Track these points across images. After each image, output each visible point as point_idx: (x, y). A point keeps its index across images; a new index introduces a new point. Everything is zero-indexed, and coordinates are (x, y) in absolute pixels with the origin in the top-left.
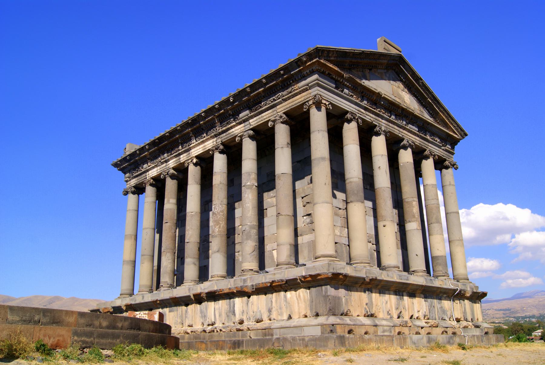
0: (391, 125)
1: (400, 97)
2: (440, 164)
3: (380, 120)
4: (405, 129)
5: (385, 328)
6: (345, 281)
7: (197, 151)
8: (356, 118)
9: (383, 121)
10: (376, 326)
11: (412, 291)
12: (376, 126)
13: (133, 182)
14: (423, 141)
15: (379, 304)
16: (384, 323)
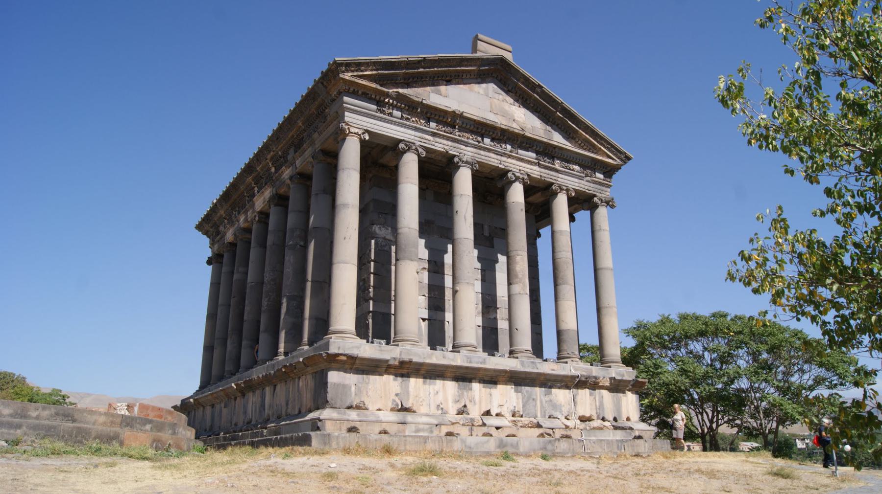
0: (482, 152)
1: (505, 114)
2: (581, 202)
3: (463, 147)
4: (510, 156)
5: (421, 426)
7: (259, 203)
8: (414, 147)
11: (491, 379)
12: (455, 156)
13: (216, 247)
14: (547, 171)
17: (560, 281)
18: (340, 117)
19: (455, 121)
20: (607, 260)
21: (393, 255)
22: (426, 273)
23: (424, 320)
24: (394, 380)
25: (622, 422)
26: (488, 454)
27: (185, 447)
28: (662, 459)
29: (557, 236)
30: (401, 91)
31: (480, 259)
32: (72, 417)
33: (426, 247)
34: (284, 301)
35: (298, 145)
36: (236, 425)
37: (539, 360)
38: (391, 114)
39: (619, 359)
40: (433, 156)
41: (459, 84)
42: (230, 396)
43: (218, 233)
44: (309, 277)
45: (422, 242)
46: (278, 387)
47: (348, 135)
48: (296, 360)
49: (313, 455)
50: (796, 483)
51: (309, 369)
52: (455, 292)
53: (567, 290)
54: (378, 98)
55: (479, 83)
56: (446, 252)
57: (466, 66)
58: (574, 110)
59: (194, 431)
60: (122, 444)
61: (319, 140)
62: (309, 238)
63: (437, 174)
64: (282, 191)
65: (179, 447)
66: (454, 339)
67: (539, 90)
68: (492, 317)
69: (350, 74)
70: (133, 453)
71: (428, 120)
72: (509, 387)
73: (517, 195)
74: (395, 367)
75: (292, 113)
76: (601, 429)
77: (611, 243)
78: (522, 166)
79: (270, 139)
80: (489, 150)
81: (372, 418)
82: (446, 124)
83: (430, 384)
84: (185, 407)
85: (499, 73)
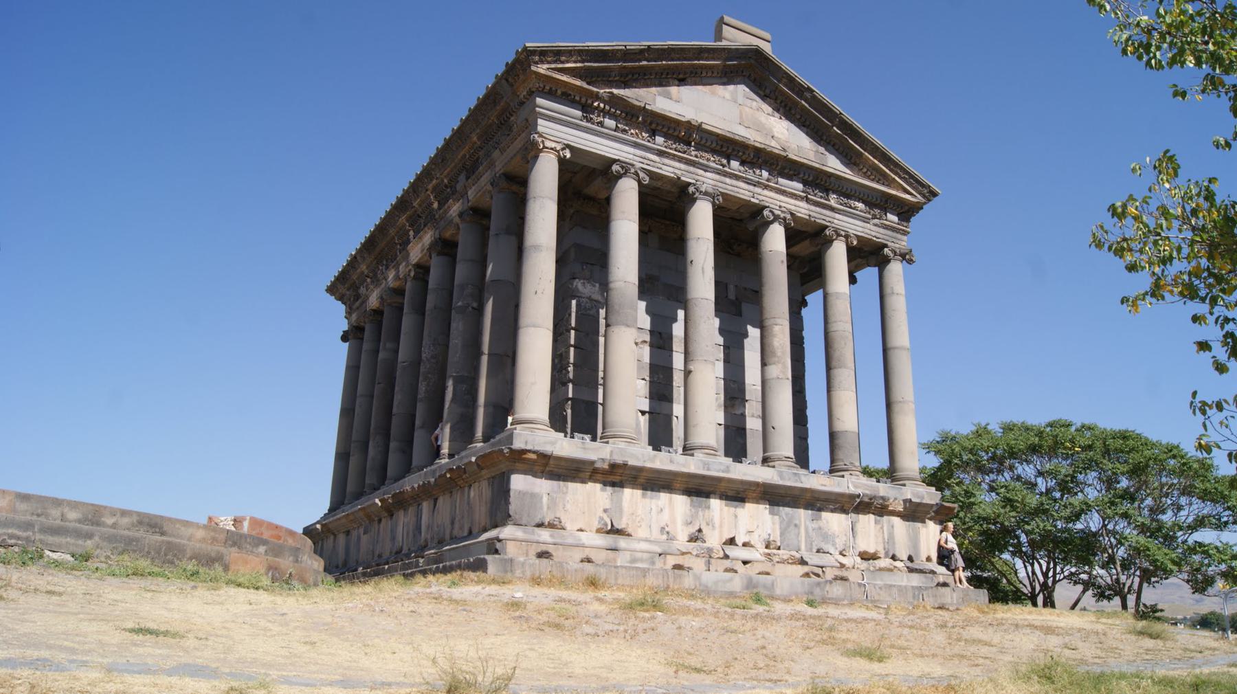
0: (728, 180)
1: (760, 128)
2: (866, 255)
3: (701, 172)
4: (766, 187)
5: (639, 555)
6: (546, 465)
7: (416, 252)
9: (708, 174)
10: (615, 550)
11: (737, 494)
12: (689, 184)
13: (354, 316)
14: (818, 209)
15: (640, 512)
16: (644, 546)
17: (834, 364)
18: (531, 126)
19: (691, 135)
20: (901, 335)
21: (602, 322)
22: (647, 349)
23: (643, 413)
24: (602, 490)
25: (920, 563)
26: (731, 594)
27: (311, 581)
28: (976, 614)
29: (831, 299)
30: (615, 91)
31: (722, 331)
32: (161, 528)
33: (648, 312)
34: (450, 383)
35: (471, 169)
36: (380, 556)
37: (803, 472)
38: (601, 124)
39: (916, 474)
40: (659, 184)
41: (696, 84)
42: (372, 518)
43: (357, 297)
44: (486, 348)
45: (642, 305)
46: (440, 501)
47: (541, 151)
48: (466, 461)
49: (489, 584)
50: (1169, 644)
51: (484, 472)
52: (687, 373)
53: (844, 376)
54: (583, 100)
55: (724, 84)
56: (676, 320)
57: (707, 59)
58: (857, 124)
59: (322, 563)
60: (226, 568)
61: (501, 161)
62: (486, 295)
63: (664, 211)
64: (447, 234)
65: (303, 580)
66: (686, 439)
67: (808, 95)
68: (739, 412)
69: (546, 66)
70: (241, 580)
71: (653, 133)
72: (761, 507)
73: (775, 241)
74: (604, 473)
75: (464, 123)
76: (890, 570)
77: (908, 312)
78: (783, 200)
79: (433, 161)
80: (737, 178)
81: (570, 541)
82: (678, 139)
83: (652, 498)
84: (308, 531)
85: (752, 70)
